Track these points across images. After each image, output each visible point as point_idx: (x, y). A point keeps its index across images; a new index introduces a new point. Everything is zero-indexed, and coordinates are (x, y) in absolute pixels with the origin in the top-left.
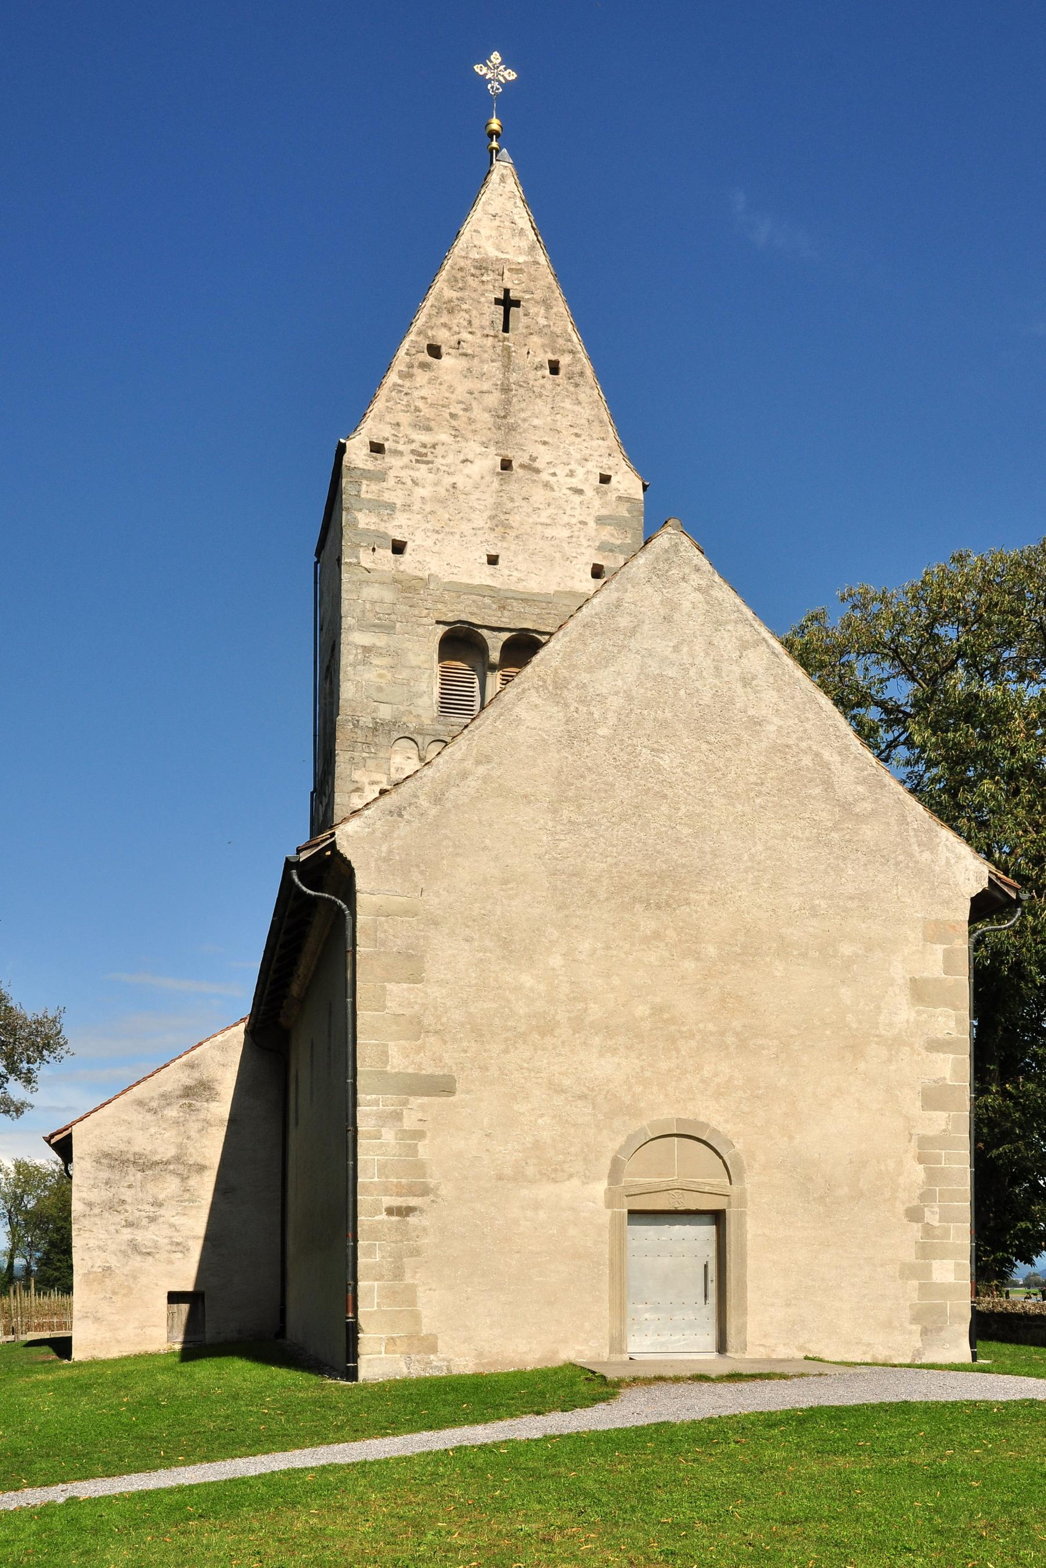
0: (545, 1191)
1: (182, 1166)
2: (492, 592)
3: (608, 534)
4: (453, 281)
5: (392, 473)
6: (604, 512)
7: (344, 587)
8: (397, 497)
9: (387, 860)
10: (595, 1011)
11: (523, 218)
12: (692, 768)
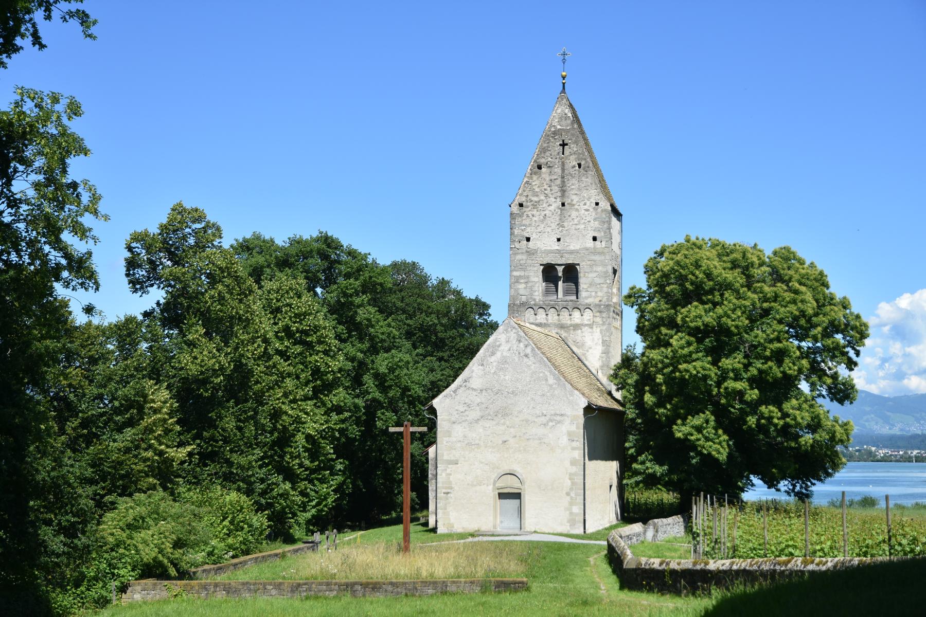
2: (558, 252)
8: (527, 222)
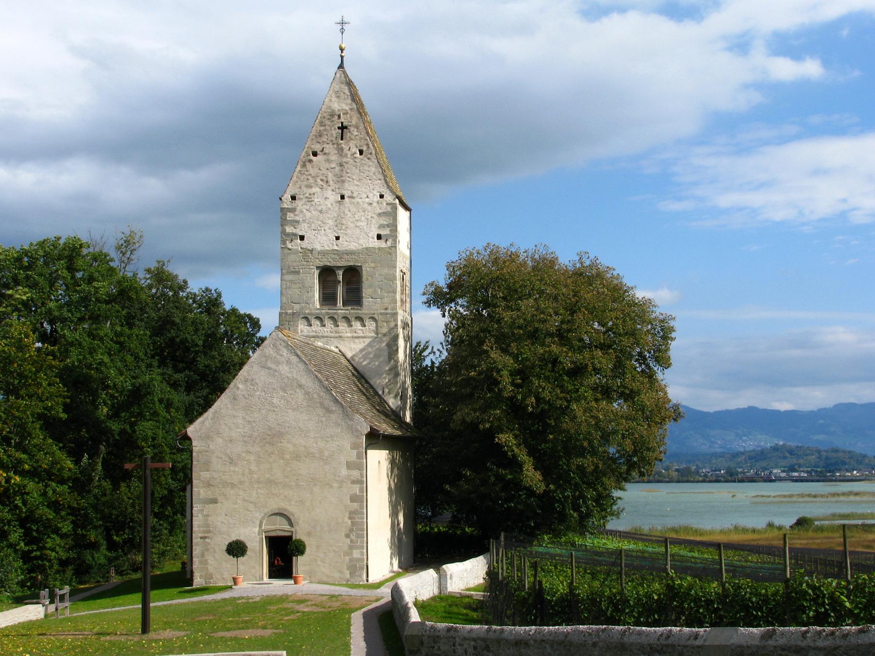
2: (334, 252)
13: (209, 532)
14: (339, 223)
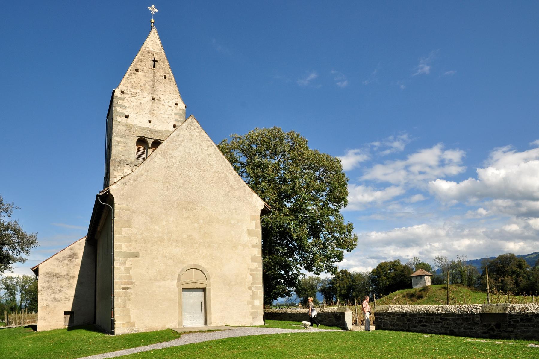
0: (162, 283)
1: (68, 276)
3: (177, 117)
4: (142, 55)
5: (126, 99)
6: (176, 112)
7: (113, 126)
8: (127, 104)
9: (122, 196)
10: (174, 236)
11: (159, 42)
12: (196, 176)
13: (132, 283)
14: (152, 113)
